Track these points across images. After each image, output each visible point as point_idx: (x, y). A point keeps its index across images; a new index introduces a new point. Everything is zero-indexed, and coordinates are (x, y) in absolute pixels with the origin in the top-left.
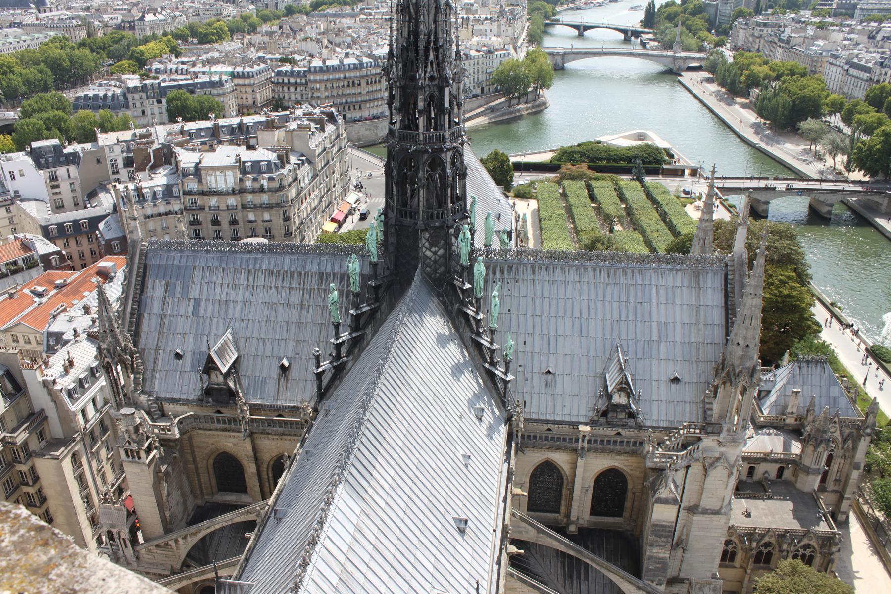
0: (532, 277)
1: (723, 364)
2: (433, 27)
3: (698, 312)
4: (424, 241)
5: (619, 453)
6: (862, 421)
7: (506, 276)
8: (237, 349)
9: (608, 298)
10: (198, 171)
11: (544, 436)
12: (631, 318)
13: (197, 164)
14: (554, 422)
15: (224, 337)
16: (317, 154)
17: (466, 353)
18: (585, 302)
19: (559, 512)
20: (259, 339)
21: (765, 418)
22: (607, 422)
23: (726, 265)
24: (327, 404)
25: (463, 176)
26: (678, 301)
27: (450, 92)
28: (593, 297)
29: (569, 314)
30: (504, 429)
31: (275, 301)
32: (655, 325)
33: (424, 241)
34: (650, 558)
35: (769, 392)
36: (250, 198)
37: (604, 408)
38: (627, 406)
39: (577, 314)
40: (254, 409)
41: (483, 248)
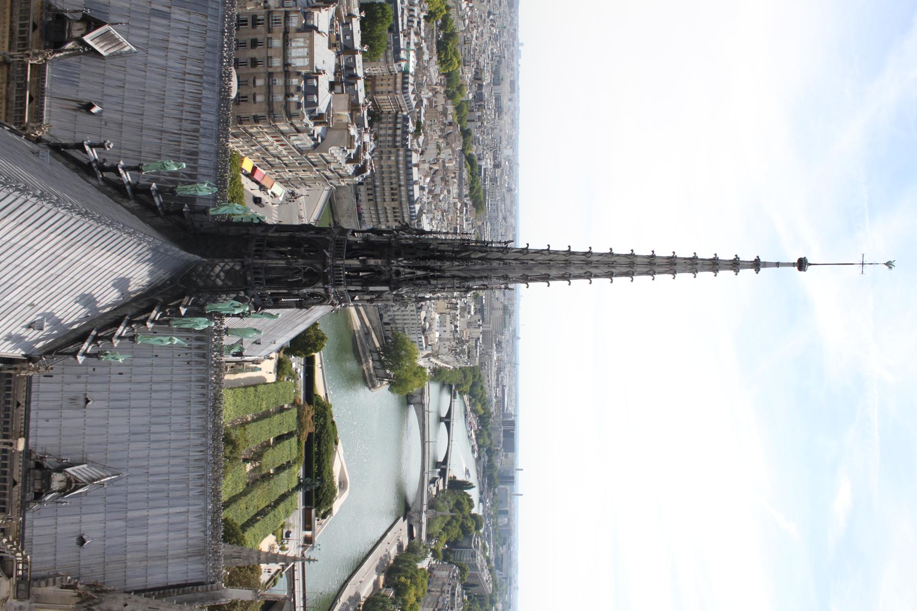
0: (193, 379)
1: (103, 591)
2: (448, 274)
3: (160, 558)
4: (231, 264)
7: (194, 351)
8: (112, 56)
9: (173, 461)
10: (310, 29)
11: (11, 399)
12: (151, 487)
13: (316, 29)
15: (126, 42)
16: (324, 154)
17: (108, 309)
18: (167, 437)
20: (123, 81)
22: (29, 469)
23: (213, 583)
24: (46, 154)
25: (300, 305)
26: (172, 535)
27: (384, 291)
28: (173, 445)
29: (154, 420)
30: (19, 353)
31: (167, 102)
32: (144, 513)
33: (231, 264)
36: (280, 82)
37: (46, 464)
39: (154, 428)
40: (39, 70)
41: (224, 327)
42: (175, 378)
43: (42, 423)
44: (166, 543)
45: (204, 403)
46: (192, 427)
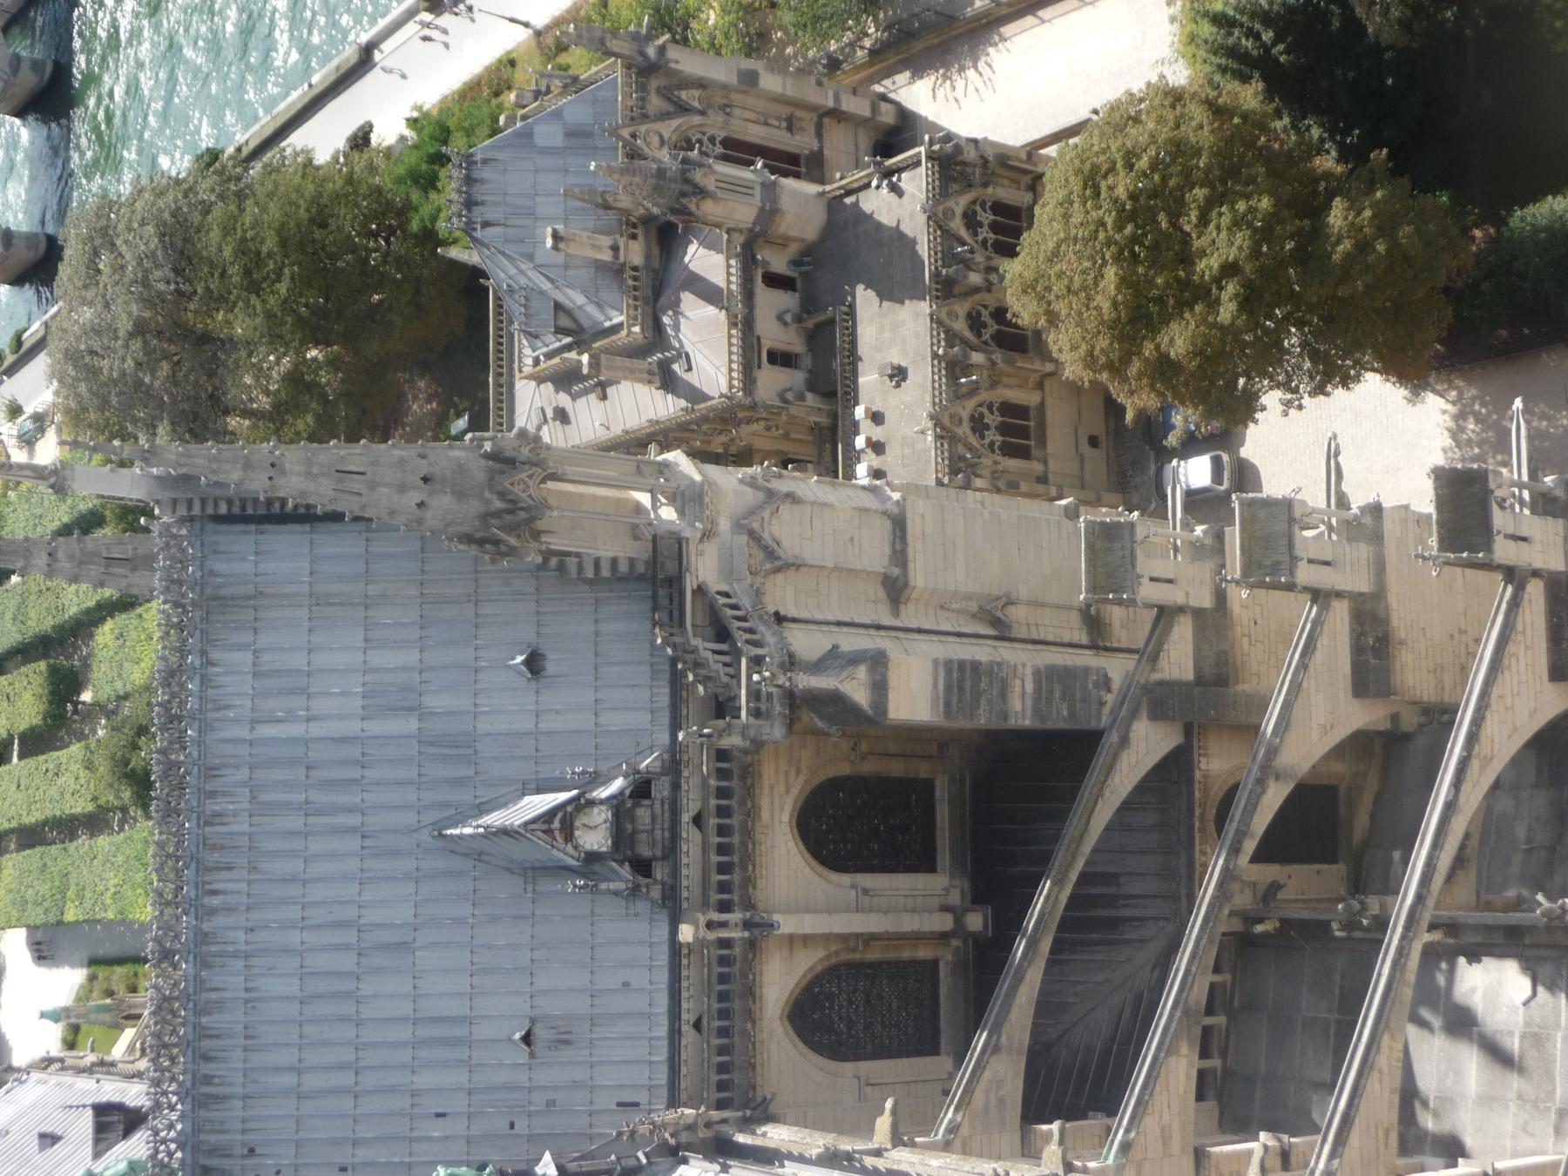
0: (239, 1104)
1: (481, 542)
5: (752, 814)
6: (628, 66)
11: (717, 1042)
18: (307, 936)
19: (934, 964)
21: (633, 320)
22: (664, 858)
26: (300, 661)
28: (294, 913)
29: (350, 985)
32: (375, 727)
34: (1036, 712)
35: (558, 307)
37: (625, 871)
38: (616, 802)
39: (348, 962)
43: (639, 978)
44: (317, 639)
45: (203, 1033)
46: (239, 964)
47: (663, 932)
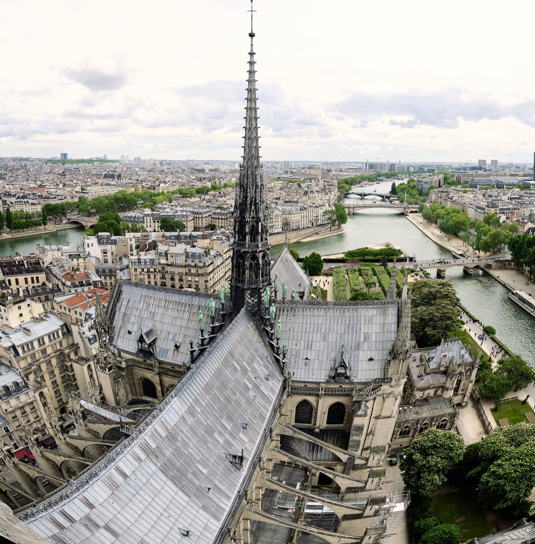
4: (247, 294)
14: (308, 382)
33: (247, 294)
39: (323, 331)
42: (301, 322)
46: (324, 314)
47: (322, 381)
